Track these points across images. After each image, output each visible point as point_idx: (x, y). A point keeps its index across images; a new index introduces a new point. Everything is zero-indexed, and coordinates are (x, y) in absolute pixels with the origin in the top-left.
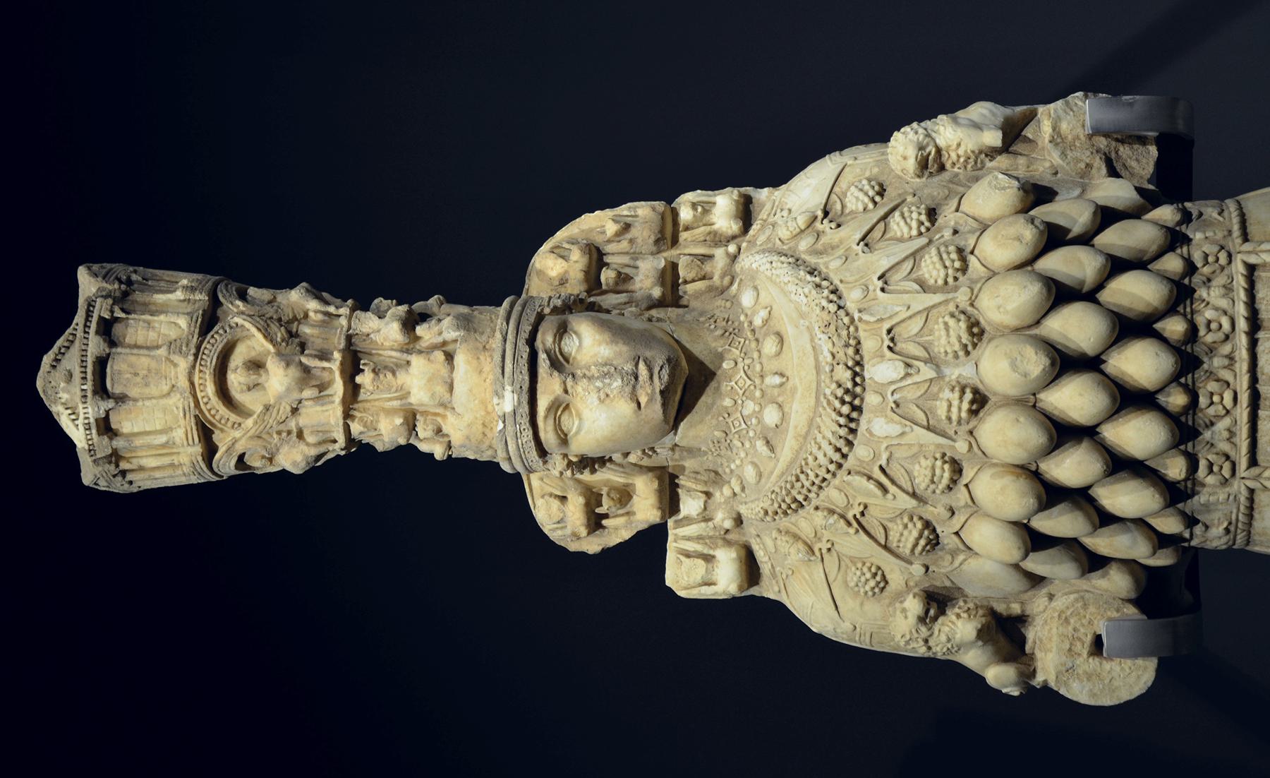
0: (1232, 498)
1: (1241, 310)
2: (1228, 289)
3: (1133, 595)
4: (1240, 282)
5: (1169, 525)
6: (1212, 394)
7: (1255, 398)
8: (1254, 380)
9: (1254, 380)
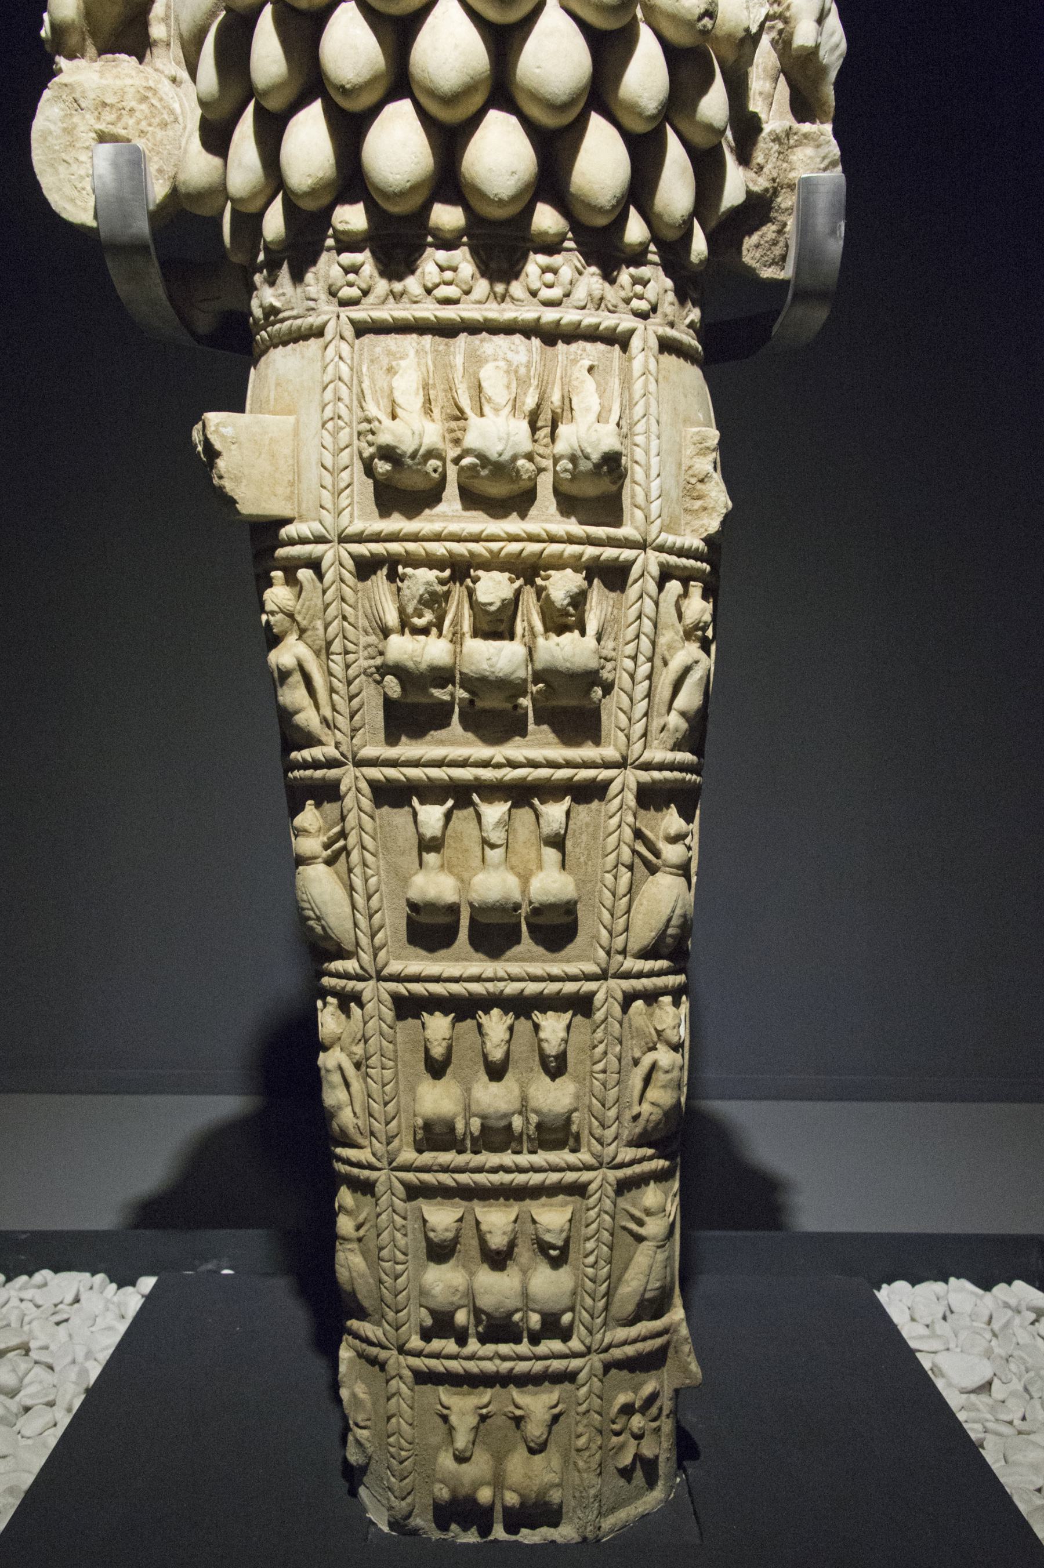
0: (312, 304)
1: (568, 316)
2: (600, 303)
3: (183, 189)
4: (606, 321)
5: (274, 223)
6: (455, 269)
7: (447, 330)
8: (473, 328)
9: (473, 328)
